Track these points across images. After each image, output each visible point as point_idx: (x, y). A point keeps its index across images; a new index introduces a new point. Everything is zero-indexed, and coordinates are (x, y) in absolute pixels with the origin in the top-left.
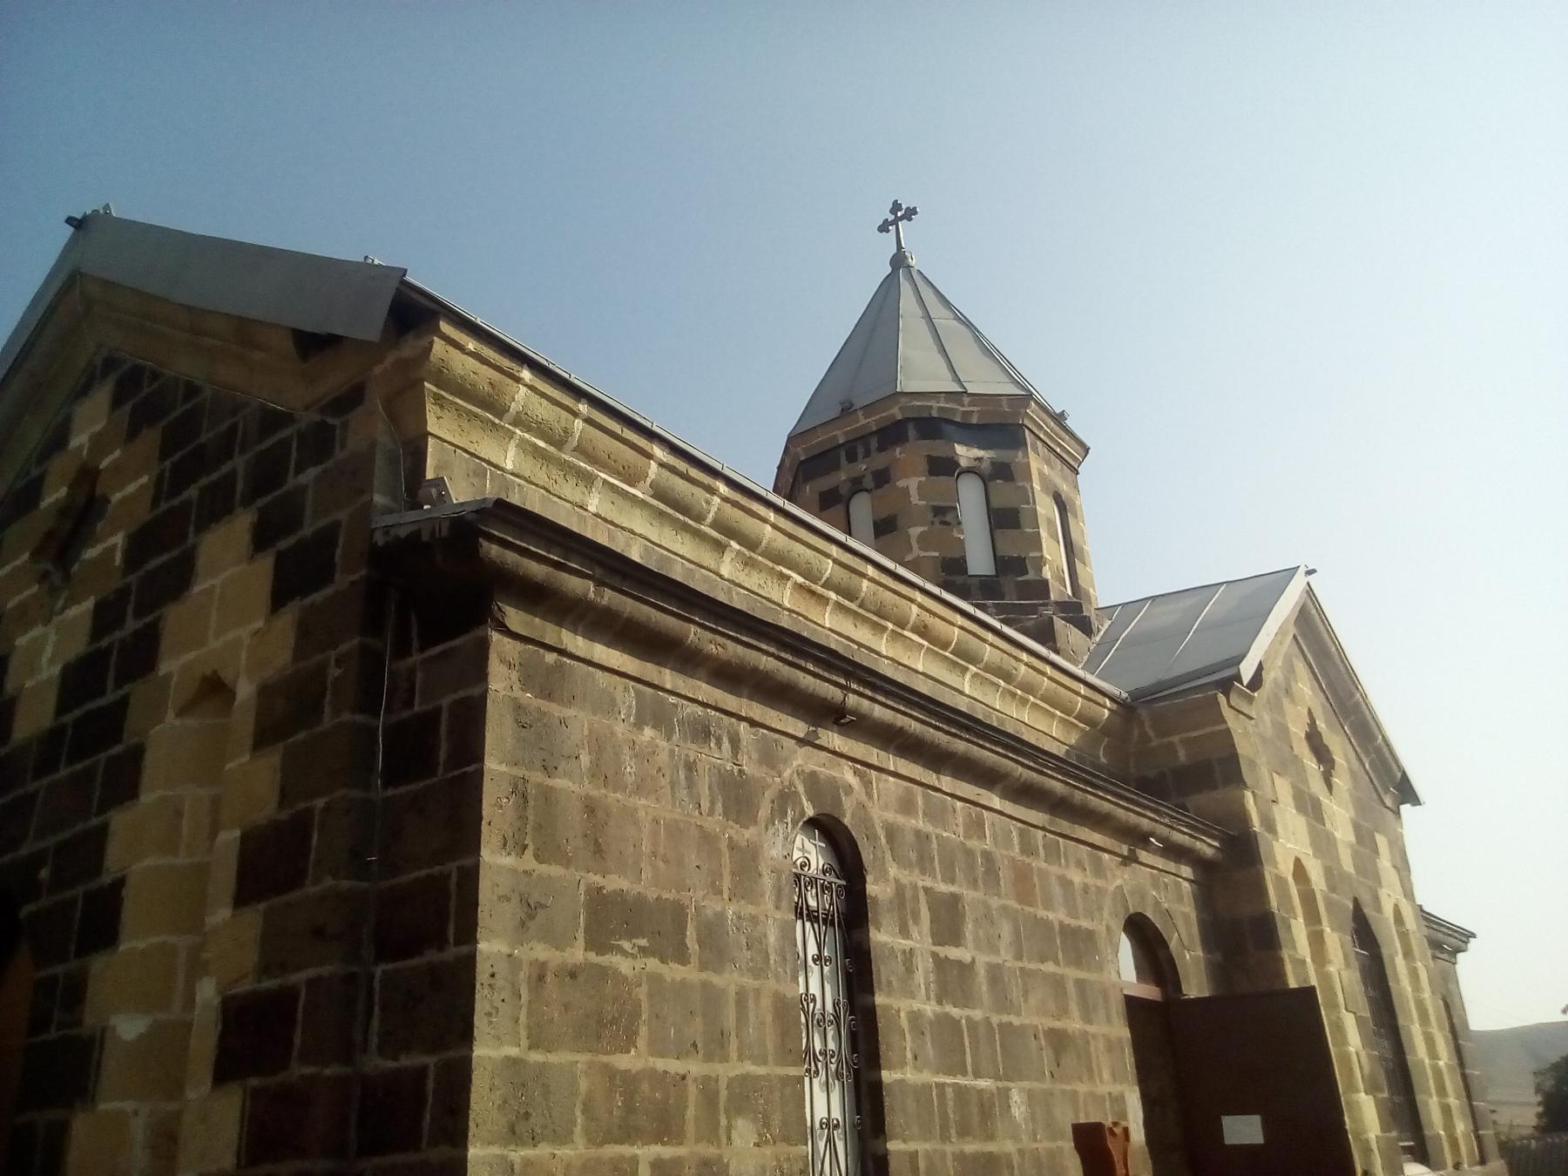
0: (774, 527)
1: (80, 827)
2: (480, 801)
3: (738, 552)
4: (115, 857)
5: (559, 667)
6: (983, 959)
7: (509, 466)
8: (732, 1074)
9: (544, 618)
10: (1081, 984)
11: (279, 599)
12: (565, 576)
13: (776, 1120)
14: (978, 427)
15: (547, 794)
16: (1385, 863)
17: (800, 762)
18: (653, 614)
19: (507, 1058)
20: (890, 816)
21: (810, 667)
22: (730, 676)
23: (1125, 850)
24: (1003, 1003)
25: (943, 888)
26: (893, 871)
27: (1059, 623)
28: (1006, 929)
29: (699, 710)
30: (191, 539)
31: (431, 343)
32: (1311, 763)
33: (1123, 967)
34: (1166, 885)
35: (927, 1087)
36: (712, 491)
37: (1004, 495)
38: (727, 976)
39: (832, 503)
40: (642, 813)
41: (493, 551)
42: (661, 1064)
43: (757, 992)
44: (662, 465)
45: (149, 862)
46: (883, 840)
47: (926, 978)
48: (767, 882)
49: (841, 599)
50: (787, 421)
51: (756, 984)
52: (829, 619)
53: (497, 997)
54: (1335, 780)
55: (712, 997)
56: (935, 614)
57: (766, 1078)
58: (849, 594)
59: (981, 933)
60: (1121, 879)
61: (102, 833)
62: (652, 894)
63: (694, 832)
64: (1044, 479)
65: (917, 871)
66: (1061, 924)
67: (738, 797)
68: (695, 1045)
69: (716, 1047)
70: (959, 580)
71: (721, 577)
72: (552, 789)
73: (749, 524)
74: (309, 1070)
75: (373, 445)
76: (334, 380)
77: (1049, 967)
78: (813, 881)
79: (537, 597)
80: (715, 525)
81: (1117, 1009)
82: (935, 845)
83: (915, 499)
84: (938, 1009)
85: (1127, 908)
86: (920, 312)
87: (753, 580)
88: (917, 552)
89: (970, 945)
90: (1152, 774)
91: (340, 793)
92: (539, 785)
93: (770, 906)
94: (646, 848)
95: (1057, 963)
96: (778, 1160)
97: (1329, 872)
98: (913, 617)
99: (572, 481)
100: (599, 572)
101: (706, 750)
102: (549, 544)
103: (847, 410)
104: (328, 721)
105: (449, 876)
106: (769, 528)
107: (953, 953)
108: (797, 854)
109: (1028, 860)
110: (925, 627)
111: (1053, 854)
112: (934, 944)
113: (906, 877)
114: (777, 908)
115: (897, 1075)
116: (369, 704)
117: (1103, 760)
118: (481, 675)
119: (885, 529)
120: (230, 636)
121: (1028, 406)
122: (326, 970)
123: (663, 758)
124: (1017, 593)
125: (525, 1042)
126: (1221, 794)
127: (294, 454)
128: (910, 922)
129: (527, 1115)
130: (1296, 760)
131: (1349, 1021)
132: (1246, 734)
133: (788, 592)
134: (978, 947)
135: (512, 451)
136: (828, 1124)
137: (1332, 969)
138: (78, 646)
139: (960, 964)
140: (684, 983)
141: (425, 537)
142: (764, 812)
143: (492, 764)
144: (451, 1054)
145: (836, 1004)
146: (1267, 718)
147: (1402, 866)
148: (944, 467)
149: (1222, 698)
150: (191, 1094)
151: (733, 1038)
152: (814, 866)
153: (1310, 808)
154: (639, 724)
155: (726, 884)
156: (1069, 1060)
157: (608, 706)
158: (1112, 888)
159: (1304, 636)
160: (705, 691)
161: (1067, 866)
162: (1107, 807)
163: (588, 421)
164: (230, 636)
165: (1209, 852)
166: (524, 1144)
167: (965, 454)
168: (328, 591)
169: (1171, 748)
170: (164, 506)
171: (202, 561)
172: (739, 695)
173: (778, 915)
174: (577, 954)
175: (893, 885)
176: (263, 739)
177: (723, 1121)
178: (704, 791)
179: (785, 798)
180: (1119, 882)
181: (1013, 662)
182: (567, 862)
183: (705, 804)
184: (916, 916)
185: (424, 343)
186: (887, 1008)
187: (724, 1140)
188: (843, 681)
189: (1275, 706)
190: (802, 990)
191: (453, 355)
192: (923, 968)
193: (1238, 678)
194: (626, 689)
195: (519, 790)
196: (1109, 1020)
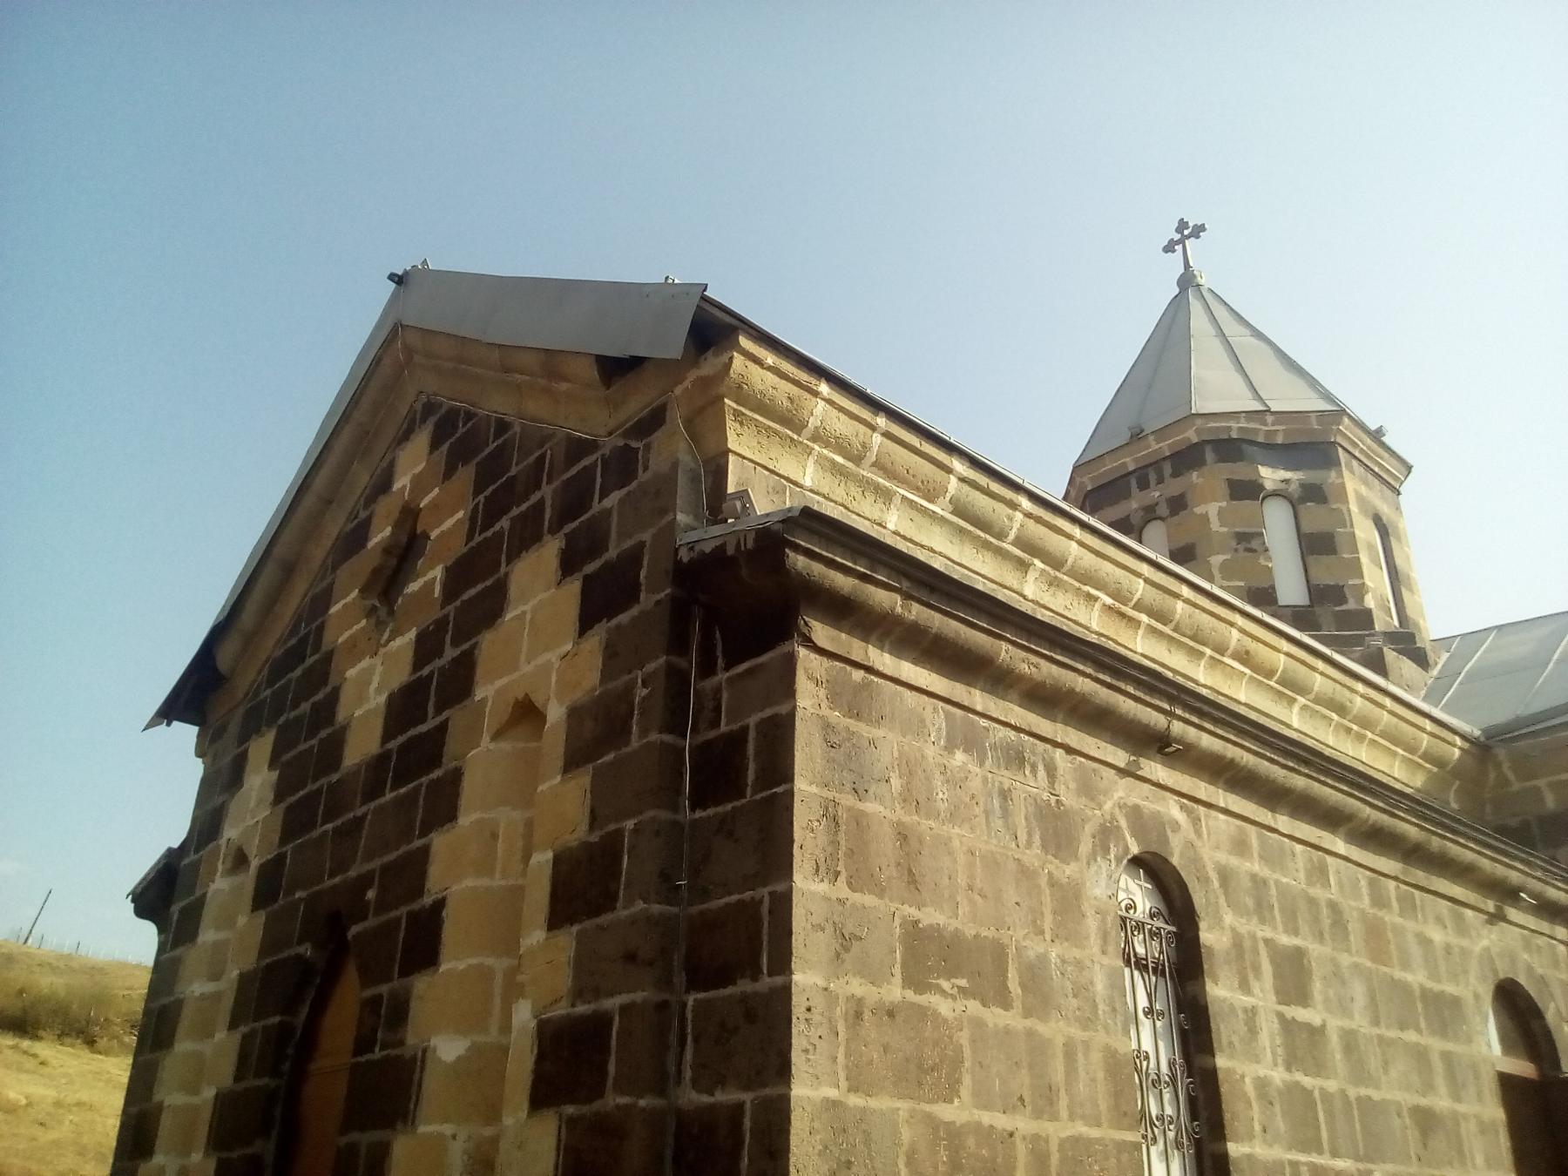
0: (1081, 544)
1: (404, 849)
2: (791, 823)
4: (436, 879)
5: (866, 685)
6: (1334, 1024)
7: (808, 483)
10: (1447, 1057)
11: (586, 623)
12: (871, 588)
14: (1285, 447)
15: (859, 819)
18: (960, 630)
19: (826, 1100)
20: (1223, 857)
21: (1131, 689)
22: (1043, 698)
23: (1490, 906)
25: (1285, 940)
26: (1229, 918)
27: (1390, 655)
28: (1358, 990)
29: (1012, 734)
30: (503, 569)
31: (731, 358)
34: (1539, 947)
35: (1279, 1165)
36: (1014, 506)
37: (1315, 517)
38: (1052, 1024)
40: (956, 843)
41: (799, 562)
42: (987, 1118)
43: (1086, 1045)
44: (963, 480)
45: (469, 882)
46: (1216, 884)
47: (1272, 1036)
48: (1092, 924)
51: (1084, 1035)
53: (814, 1033)
55: (1038, 1048)
57: (1098, 1141)
58: (1161, 616)
59: (1331, 992)
60: (1488, 939)
61: (424, 853)
62: (970, 931)
63: (1012, 866)
64: (1362, 500)
65: (1255, 920)
67: (1057, 830)
68: (1021, 1099)
69: (1045, 1102)
71: (1024, 597)
72: (863, 813)
73: (1054, 542)
74: (623, 1100)
75: (675, 466)
76: (636, 404)
77: (1411, 1036)
78: (1140, 926)
79: (843, 611)
80: (1020, 542)
82: (1273, 891)
83: (1215, 525)
84: (1287, 1076)
85: (1495, 972)
86: (1213, 331)
89: (1320, 1007)
91: (651, 813)
92: (850, 809)
93: (1096, 950)
94: (962, 880)
95: (1419, 1031)
98: (1233, 644)
99: (870, 498)
100: (906, 585)
101: (1020, 777)
102: (855, 554)
103: (1137, 436)
104: (635, 743)
105: (761, 901)
106: (1074, 545)
108: (1122, 895)
109: (1380, 914)
110: (1247, 652)
111: (1408, 908)
114: (1104, 952)
116: (675, 724)
117: (1454, 806)
118: (790, 692)
120: (541, 660)
122: (639, 996)
123: (975, 784)
125: (843, 1084)
127: (599, 480)
128: (1251, 977)
129: (849, 1164)
133: (1096, 613)
134: (1328, 1010)
135: (811, 467)
138: (401, 675)
140: (1007, 1031)
141: (730, 551)
142: (1085, 847)
143: (803, 785)
144: (768, 1091)
145: (1171, 1064)
150: (508, 1121)
151: (1062, 1093)
152: (1140, 908)
154: (950, 748)
155: (1048, 923)
157: (917, 727)
158: (1477, 949)
162: (1468, 856)
164: (541, 660)
167: (1270, 476)
168: (635, 611)
170: (478, 539)
171: (513, 590)
173: (1106, 961)
174: (895, 992)
175: (1228, 933)
176: (572, 763)
179: (1107, 833)
180: (1485, 942)
181: (1347, 693)
182: (881, 892)
184: (1257, 969)
185: (725, 358)
186: (1229, 1071)
188: (1167, 707)
190: (1134, 1046)
191: (751, 369)
192: (1268, 1029)
194: (935, 709)
195: (831, 815)
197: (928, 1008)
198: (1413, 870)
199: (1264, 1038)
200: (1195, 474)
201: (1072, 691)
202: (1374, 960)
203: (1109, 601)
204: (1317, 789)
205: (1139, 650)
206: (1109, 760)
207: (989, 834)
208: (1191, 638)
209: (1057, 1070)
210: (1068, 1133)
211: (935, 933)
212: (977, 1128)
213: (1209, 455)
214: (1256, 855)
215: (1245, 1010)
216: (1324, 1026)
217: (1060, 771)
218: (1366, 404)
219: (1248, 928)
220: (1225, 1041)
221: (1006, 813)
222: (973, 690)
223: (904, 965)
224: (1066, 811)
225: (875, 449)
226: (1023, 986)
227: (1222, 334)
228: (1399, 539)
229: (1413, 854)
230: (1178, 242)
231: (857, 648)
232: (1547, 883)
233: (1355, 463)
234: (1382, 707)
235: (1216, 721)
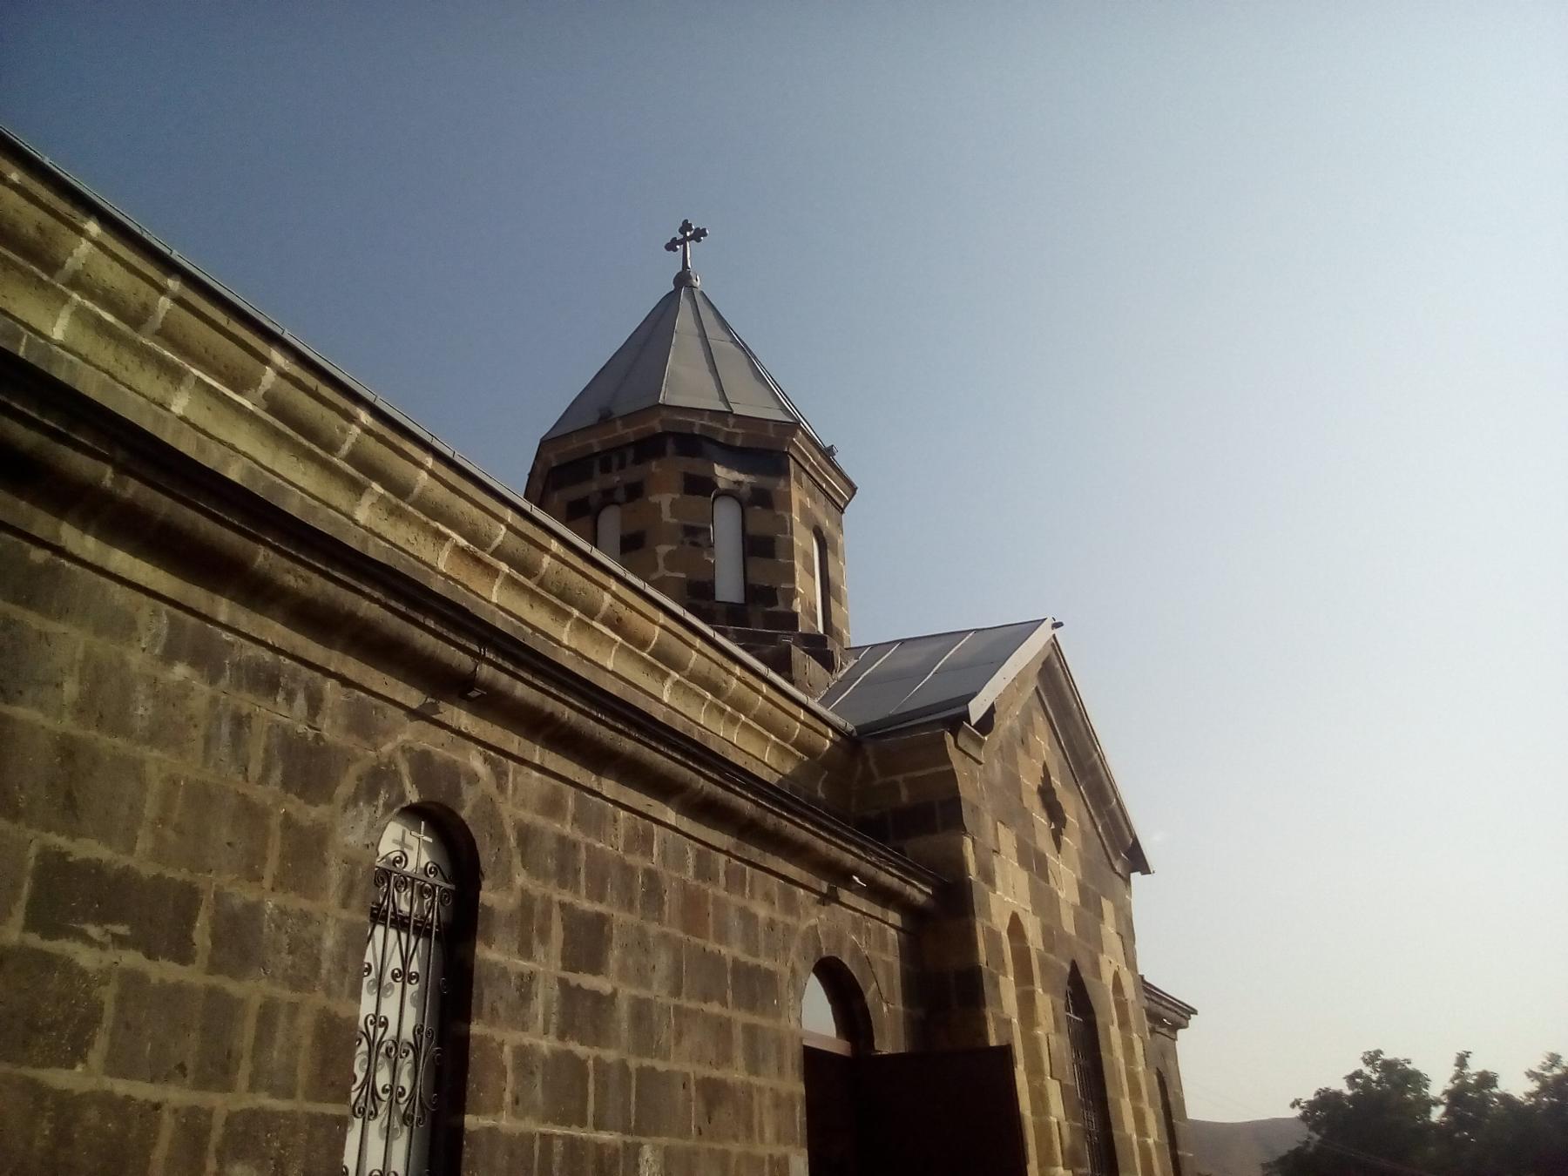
0: (431, 473)
3: (381, 497)
7: (58, 333)
8: (236, 1107)
9: (34, 502)
10: (751, 1031)
16: (1109, 929)
20: (527, 816)
21: (431, 623)
24: (645, 1040)
25: (586, 905)
26: (521, 879)
27: (797, 653)
28: (663, 961)
29: (268, 656)
32: (1041, 818)
33: (816, 1017)
36: (351, 419)
37: (761, 522)
39: (579, 513)
40: (151, 769)
42: (121, 1087)
43: (294, 1008)
44: (282, 374)
46: (513, 842)
48: (335, 873)
49: (515, 574)
50: (544, 424)
51: (294, 997)
52: (496, 594)
54: (1065, 838)
55: (222, 1010)
56: (632, 608)
58: (528, 569)
59: (630, 961)
60: (815, 918)
62: (148, 870)
65: (554, 881)
66: (735, 960)
67: (308, 768)
68: (182, 1067)
69: (218, 1071)
70: (704, 604)
71: (356, 522)
77: (714, 1008)
78: (405, 882)
80: (352, 458)
81: (792, 1059)
82: (583, 855)
83: (666, 516)
84: (558, 1045)
85: (819, 950)
87: (400, 533)
88: (662, 571)
94: (150, 810)
95: (724, 1003)
97: (1048, 933)
98: (605, 607)
100: (120, 455)
101: (269, 704)
103: (606, 419)
106: (424, 475)
107: (588, 981)
108: (388, 846)
109: (703, 886)
110: (619, 619)
111: (735, 882)
112: (564, 969)
113: (537, 888)
114: (345, 905)
115: (486, 1122)
117: (821, 794)
119: (632, 546)
121: (794, 434)
124: (764, 621)
128: (535, 942)
130: (1025, 814)
131: (1054, 1090)
132: (973, 780)
137: (1040, 1032)
139: (597, 997)
140: (179, 988)
142: (345, 788)
145: (418, 1031)
146: (997, 766)
147: (1127, 935)
148: (701, 486)
149: (949, 738)
153: (1034, 863)
154: (170, 655)
155: (271, 868)
158: (803, 926)
159: (1046, 690)
160: (277, 631)
161: (752, 897)
162: (804, 836)
163: (179, 301)
167: (724, 475)
169: (894, 787)
172: (328, 643)
173: (345, 915)
178: (256, 751)
179: (377, 779)
180: (813, 921)
181: (724, 675)
183: (255, 769)
184: (544, 935)
186: (484, 1040)
188: (475, 648)
189: (1007, 754)
192: (544, 998)
193: (966, 716)
194: (156, 613)
196: (780, 1069)
197: (59, 957)
198: (747, 846)
199: (538, 1006)
200: (654, 463)
201: (351, 617)
202: (687, 931)
203: (463, 542)
205: (494, 600)
206: (399, 699)
208: (558, 596)
211: (94, 870)
213: (670, 447)
214: (569, 818)
215: (521, 976)
216: (614, 994)
218: (822, 424)
219: (543, 890)
220: (486, 1005)
221: (237, 738)
222: (217, 597)
225: (162, 314)
226: (217, 939)
227: (703, 336)
228: (836, 554)
229: (747, 830)
230: (680, 242)
231: (42, 523)
233: (804, 476)
234: (759, 692)
235: (536, 672)
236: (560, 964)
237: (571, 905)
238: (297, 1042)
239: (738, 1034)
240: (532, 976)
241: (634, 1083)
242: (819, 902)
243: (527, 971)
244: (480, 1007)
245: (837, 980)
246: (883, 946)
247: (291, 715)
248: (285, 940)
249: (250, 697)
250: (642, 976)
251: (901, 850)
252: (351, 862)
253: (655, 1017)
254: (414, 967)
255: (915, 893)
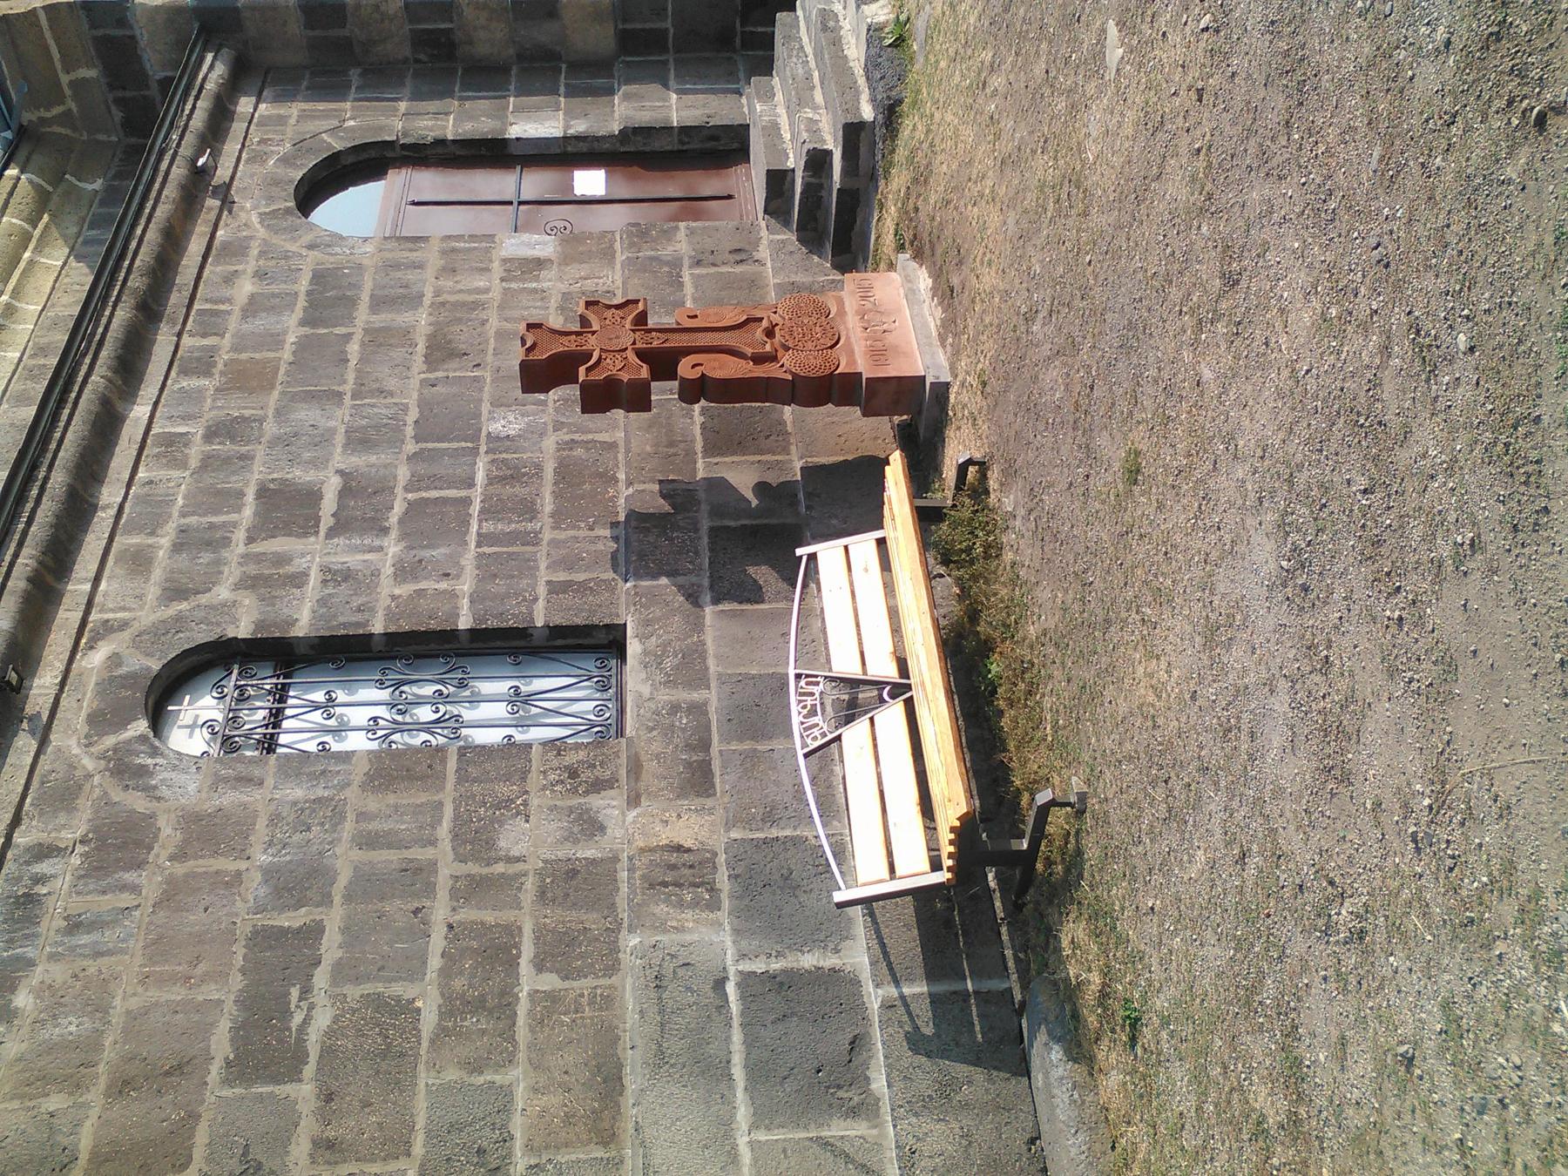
8: (451, 856)
10: (377, 304)
13: (504, 790)
17: (73, 742)
20: (153, 592)
23: (213, 203)
25: (248, 512)
26: (223, 593)
28: (306, 415)
34: (262, 141)
38: (339, 864)
40: (134, 1003)
42: (435, 962)
43: (362, 816)
46: (184, 606)
48: (229, 798)
51: (351, 816)
55: (367, 886)
60: (252, 214)
62: (237, 981)
65: (225, 554)
66: (303, 323)
67: (119, 845)
68: (416, 912)
69: (418, 877)
77: (354, 348)
78: (233, 720)
82: (193, 520)
84: (394, 534)
85: (288, 211)
90: (118, 115)
94: (177, 994)
96: (544, 788)
107: (329, 505)
109: (220, 366)
111: (212, 324)
112: (317, 533)
117: (98, 184)
123: (58, 973)
125: (402, 1164)
126: (143, 38)
128: (290, 569)
129: (481, 1152)
136: (518, 699)
139: (345, 493)
140: (345, 930)
142: (138, 802)
145: (381, 684)
155: (229, 865)
156: (462, 336)
158: (262, 232)
161: (229, 300)
162: (153, 235)
165: (220, 69)
166: (509, 1155)
173: (270, 782)
174: (304, 1092)
177: (500, 868)
179: (124, 768)
180: (255, 219)
182: (194, 1117)
183: (126, 899)
184: (281, 559)
187: (520, 867)
192: (347, 554)
196: (420, 266)
199: (354, 560)
202: (273, 387)
204: (68, 453)
206: (29, 760)
207: (123, 951)
209: (388, 857)
210: (449, 848)
211: (241, 1034)
212: (445, 973)
214: (150, 541)
215: (324, 582)
216: (340, 472)
217: (43, 837)
220: (358, 618)
223: (276, 1080)
224: (95, 830)
226: (299, 905)
229: (150, 310)
232: (186, 126)
236: (312, 539)
237: (248, 530)
238: (389, 809)
239: (382, 319)
240: (326, 569)
241: (430, 445)
242: (230, 212)
243: (321, 577)
244: (358, 624)
245: (316, 188)
246: (282, 120)
247: (61, 876)
248: (297, 837)
249: (45, 924)
250: (324, 439)
251: (166, 83)
252: (217, 782)
253: (364, 422)
254: (319, 696)
255: (214, 75)
